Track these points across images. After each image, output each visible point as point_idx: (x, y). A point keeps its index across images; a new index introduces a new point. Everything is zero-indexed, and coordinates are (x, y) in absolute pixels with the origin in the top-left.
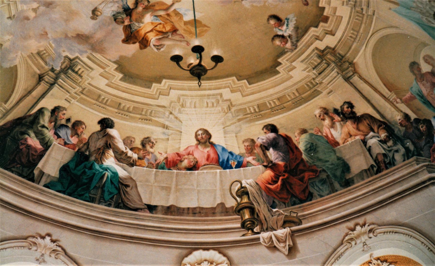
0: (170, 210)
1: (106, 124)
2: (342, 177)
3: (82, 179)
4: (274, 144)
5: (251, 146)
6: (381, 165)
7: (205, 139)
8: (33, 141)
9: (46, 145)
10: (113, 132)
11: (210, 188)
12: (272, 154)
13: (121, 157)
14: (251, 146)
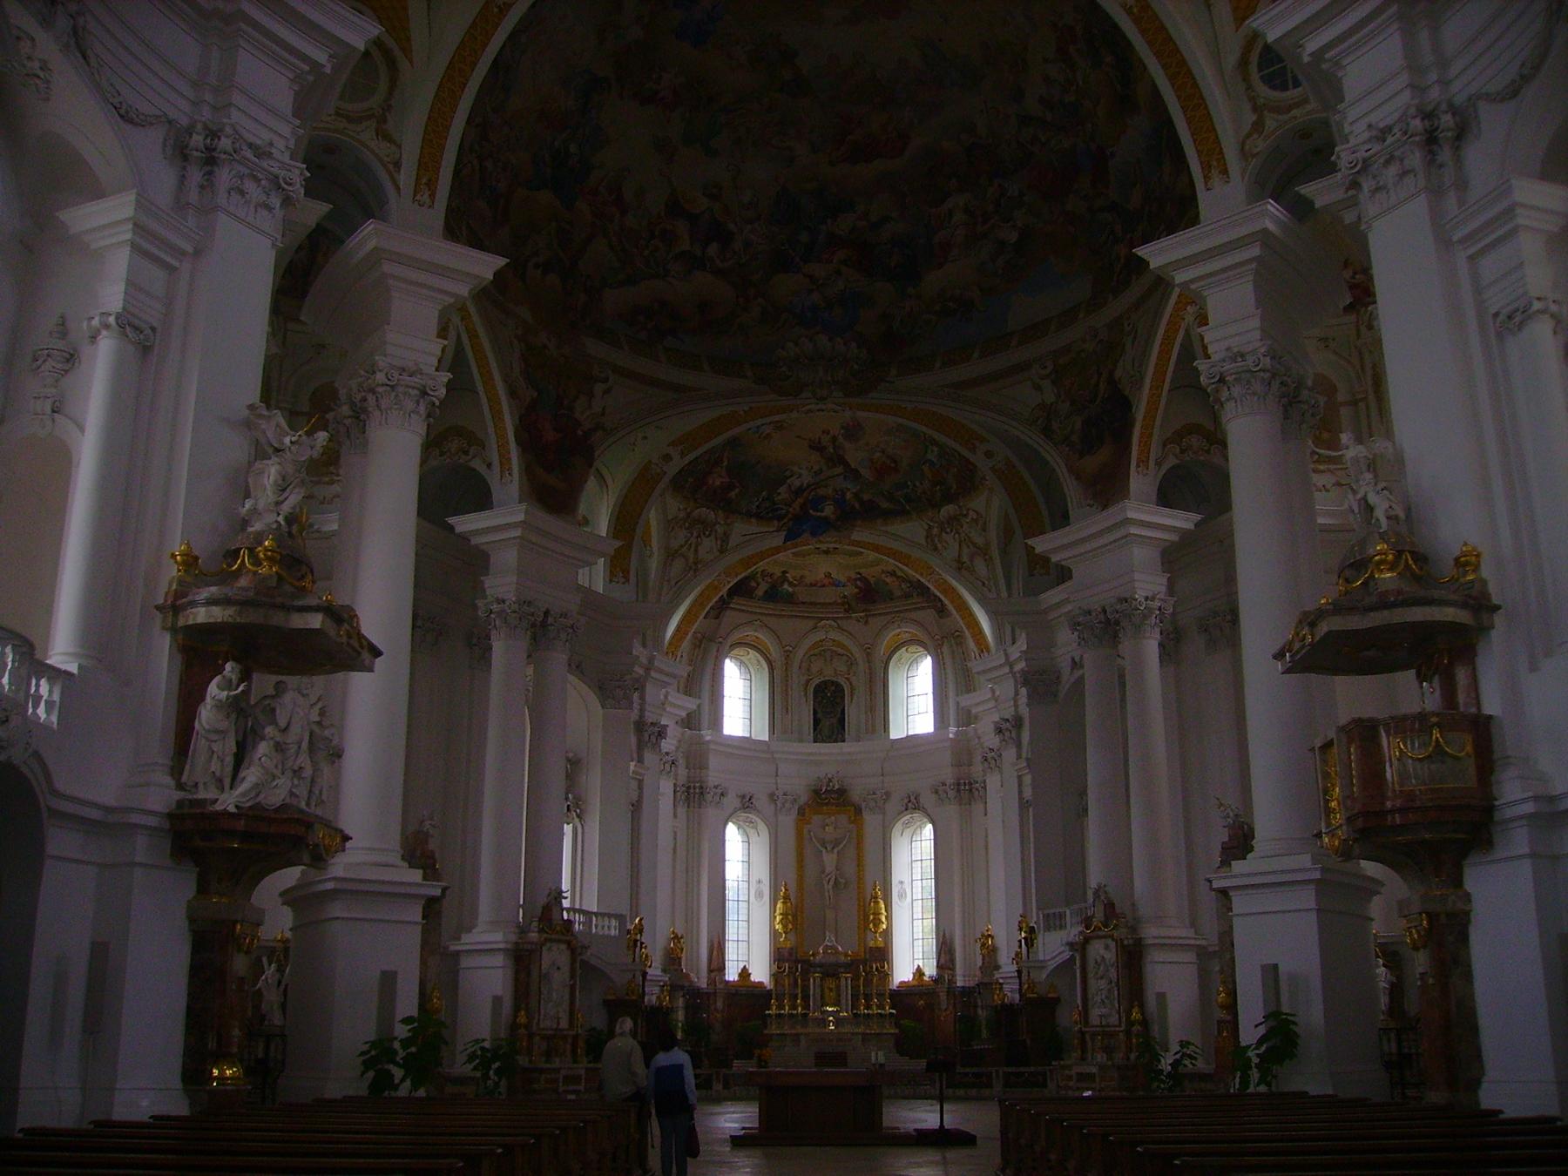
3: (773, 595)
6: (907, 596)
7: (828, 575)
8: (753, 584)
11: (829, 595)
13: (791, 584)
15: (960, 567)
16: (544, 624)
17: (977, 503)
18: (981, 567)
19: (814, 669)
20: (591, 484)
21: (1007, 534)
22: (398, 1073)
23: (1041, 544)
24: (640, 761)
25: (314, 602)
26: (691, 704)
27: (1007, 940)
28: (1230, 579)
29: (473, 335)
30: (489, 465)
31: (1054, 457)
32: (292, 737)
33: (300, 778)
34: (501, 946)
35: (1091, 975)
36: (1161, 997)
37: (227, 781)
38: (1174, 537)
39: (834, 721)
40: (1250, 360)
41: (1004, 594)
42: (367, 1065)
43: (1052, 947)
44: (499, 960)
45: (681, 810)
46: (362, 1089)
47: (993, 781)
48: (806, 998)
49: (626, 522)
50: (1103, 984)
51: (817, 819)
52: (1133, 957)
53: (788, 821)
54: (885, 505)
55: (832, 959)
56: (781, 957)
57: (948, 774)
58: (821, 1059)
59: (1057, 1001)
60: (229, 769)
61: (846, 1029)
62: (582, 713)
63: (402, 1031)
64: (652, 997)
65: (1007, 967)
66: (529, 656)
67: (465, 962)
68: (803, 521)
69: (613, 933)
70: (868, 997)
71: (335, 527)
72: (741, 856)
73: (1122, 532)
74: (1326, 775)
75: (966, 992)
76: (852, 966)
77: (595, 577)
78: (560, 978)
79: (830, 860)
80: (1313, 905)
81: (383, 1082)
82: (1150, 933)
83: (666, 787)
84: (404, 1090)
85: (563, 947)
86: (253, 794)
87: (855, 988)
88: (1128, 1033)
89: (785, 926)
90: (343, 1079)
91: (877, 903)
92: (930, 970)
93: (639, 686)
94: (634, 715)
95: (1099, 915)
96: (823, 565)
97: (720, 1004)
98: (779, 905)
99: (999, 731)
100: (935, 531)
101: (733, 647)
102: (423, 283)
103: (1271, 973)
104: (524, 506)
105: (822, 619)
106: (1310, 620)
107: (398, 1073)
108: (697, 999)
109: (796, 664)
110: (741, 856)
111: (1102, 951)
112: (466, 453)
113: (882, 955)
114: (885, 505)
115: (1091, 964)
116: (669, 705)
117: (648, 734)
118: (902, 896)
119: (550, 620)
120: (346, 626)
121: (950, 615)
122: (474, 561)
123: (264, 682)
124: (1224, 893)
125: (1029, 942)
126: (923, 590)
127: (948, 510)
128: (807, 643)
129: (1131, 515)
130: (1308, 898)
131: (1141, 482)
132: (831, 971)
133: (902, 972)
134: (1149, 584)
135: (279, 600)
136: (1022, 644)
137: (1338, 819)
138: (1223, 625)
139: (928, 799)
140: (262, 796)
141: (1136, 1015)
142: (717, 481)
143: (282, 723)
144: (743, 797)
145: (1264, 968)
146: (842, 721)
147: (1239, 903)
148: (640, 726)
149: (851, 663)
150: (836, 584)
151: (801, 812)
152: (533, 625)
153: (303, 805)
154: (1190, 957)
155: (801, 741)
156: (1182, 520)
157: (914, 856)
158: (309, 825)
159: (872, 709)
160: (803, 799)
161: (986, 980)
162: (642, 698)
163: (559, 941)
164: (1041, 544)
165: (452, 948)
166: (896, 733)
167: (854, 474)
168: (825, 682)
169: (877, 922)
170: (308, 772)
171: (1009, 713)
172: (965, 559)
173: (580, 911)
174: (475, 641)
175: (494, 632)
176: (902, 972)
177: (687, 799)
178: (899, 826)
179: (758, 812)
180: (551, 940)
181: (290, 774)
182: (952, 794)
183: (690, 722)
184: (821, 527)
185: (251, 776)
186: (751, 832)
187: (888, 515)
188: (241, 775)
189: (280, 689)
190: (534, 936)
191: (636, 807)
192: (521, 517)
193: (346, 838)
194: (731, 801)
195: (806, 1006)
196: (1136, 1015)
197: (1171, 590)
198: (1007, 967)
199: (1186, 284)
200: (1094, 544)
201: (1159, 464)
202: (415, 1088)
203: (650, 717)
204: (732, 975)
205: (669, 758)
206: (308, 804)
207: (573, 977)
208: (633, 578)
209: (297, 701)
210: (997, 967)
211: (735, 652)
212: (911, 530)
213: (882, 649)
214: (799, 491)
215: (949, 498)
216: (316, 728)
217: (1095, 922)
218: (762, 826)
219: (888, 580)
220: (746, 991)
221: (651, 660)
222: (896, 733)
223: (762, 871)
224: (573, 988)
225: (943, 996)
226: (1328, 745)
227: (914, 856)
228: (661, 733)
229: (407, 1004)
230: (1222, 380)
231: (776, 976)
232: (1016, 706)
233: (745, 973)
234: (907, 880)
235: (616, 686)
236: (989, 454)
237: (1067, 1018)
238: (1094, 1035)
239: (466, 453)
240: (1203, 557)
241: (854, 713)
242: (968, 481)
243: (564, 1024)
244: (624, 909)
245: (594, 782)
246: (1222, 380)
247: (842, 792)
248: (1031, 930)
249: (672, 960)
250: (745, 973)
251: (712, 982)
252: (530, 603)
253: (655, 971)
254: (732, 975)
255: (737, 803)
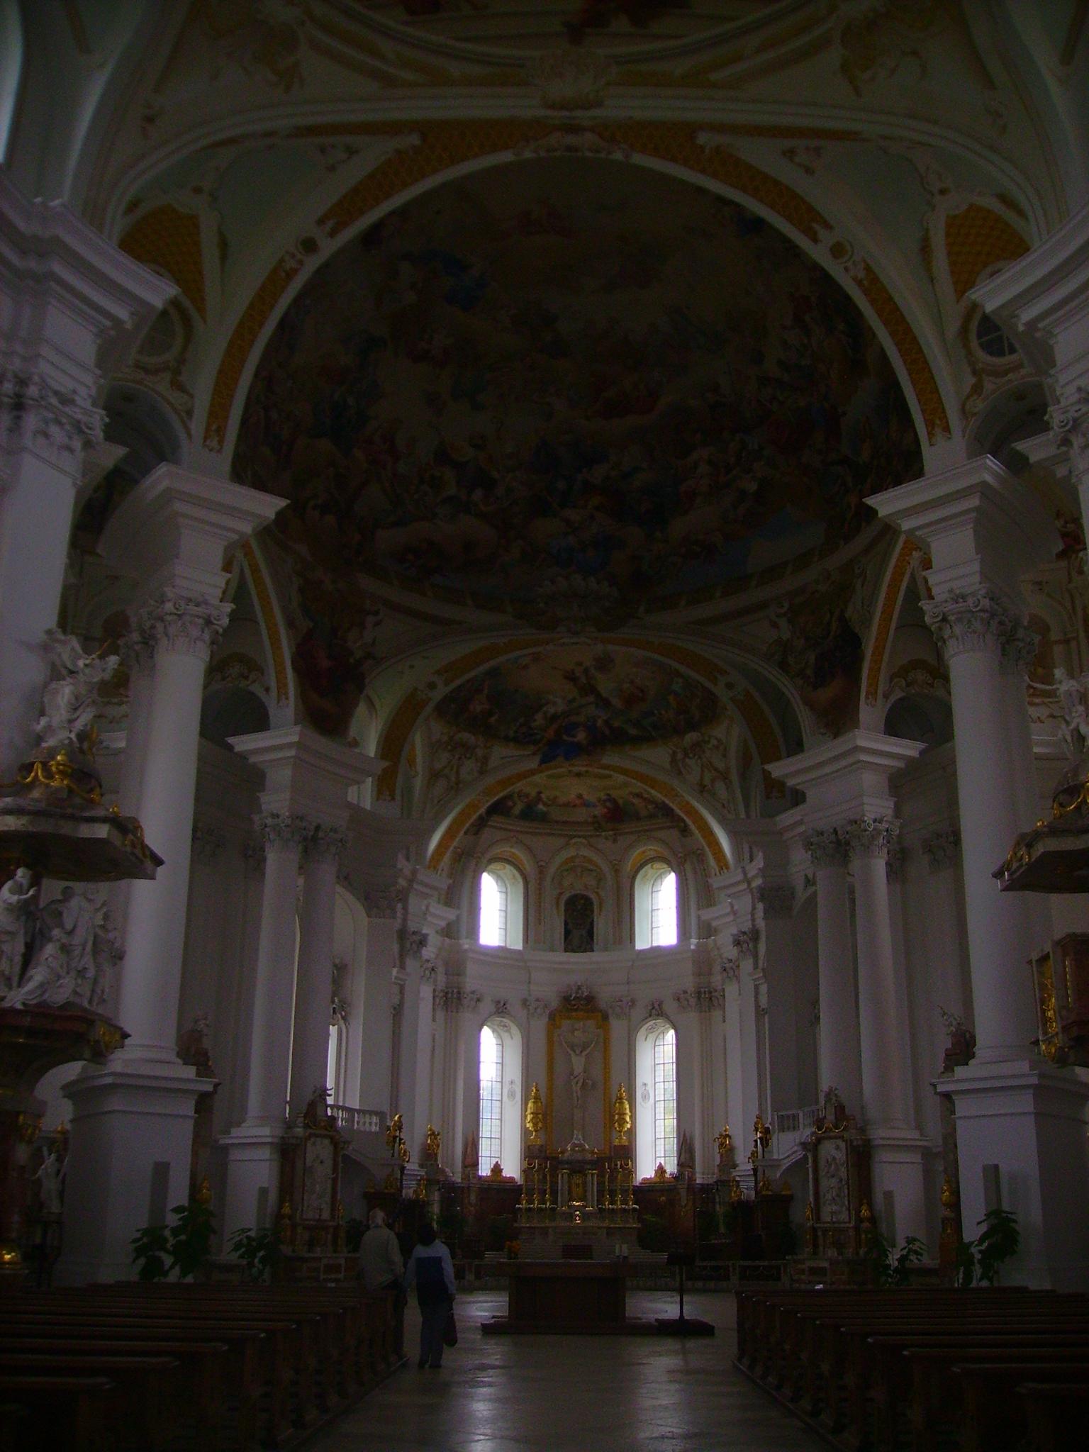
0: (565, 823)
1: (540, 793)
2: (638, 819)
3: (529, 814)
4: (609, 800)
5: (599, 800)
6: (652, 816)
7: (580, 796)
8: (510, 803)
9: (515, 804)
10: (543, 796)
11: (582, 814)
12: (608, 804)
13: (545, 804)
14: (599, 800)
15: (702, 789)
16: (314, 839)
17: (719, 731)
18: (720, 787)
19: (566, 883)
20: (361, 709)
21: (746, 760)
22: (168, 1260)
23: (778, 769)
24: (402, 967)
25: (101, 813)
26: (451, 914)
27: (744, 1142)
28: (952, 803)
29: (255, 570)
30: (267, 690)
31: (789, 688)
32: (77, 940)
33: (84, 977)
34: (269, 1140)
35: (822, 1173)
36: (889, 1195)
37: (15, 979)
38: (901, 764)
39: (584, 933)
40: (970, 601)
41: (743, 816)
42: (140, 1252)
43: (786, 1147)
44: (266, 1153)
45: (440, 1015)
46: (133, 1275)
47: (731, 990)
48: (554, 1193)
49: (393, 745)
50: (833, 1182)
51: (566, 1023)
52: (862, 1158)
53: (540, 1024)
54: (633, 731)
55: (579, 1156)
56: (531, 1154)
57: (689, 983)
58: (569, 1251)
59: (789, 1199)
60: (17, 969)
61: (592, 1223)
62: (348, 920)
63: (172, 1220)
64: (409, 1192)
65: (744, 1165)
66: (301, 868)
67: (235, 1155)
68: (559, 745)
69: (374, 1128)
70: (612, 1193)
71: (122, 744)
72: (495, 1057)
73: (851, 760)
74: (1043, 987)
75: (705, 1188)
76: (598, 1163)
77: (364, 794)
78: (323, 1171)
79: (578, 1063)
80: (1031, 1109)
81: (152, 1269)
82: (879, 1134)
83: (426, 992)
84: (173, 1277)
85: (327, 1142)
86: (39, 992)
87: (601, 1184)
88: (857, 1228)
89: (535, 1125)
90: (115, 1265)
91: (621, 1103)
92: (671, 1168)
93: (403, 897)
94: (397, 924)
95: (831, 1117)
96: (574, 786)
97: (473, 1198)
98: (530, 1105)
99: (737, 943)
100: (680, 756)
101: (491, 861)
102: (210, 520)
103: (992, 1173)
104: (298, 728)
105: (572, 837)
106: (1027, 841)
107: (168, 1260)
108: (452, 1193)
109: (549, 879)
110: (495, 1057)
111: (833, 1151)
112: (247, 678)
113: (627, 1153)
114: (633, 731)
115: (822, 1164)
116: (430, 916)
117: (409, 942)
118: (645, 1097)
119: (321, 834)
120: (131, 837)
121: (692, 834)
122: (251, 778)
123: (52, 888)
124: (947, 1096)
125: (765, 1141)
126: (668, 812)
127: (691, 737)
128: (559, 859)
129: (861, 743)
130: (1026, 1103)
131: (870, 713)
132: (578, 1168)
133: (645, 1170)
134: (877, 807)
135: (69, 811)
136: (759, 862)
137: (1055, 1027)
138: (946, 845)
139: (670, 1006)
140: (47, 995)
141: (864, 1212)
142: (478, 706)
143: (69, 927)
144: (499, 1002)
145: (985, 1168)
146: (591, 934)
147: (962, 1107)
148: (402, 934)
149: (600, 879)
150: (586, 804)
151: (552, 1017)
152: (305, 839)
153: (86, 1004)
154: (917, 1158)
155: (552, 950)
156: (909, 749)
157: (657, 1060)
158: (91, 1023)
159: (618, 923)
160: (555, 1004)
161: (724, 1178)
162: (405, 909)
163: (325, 1136)
164: (778, 769)
165: (222, 1142)
166: (641, 944)
167: (605, 703)
168: (575, 896)
169: (622, 1121)
170: (91, 973)
171: (747, 926)
172: (707, 781)
173: (344, 1108)
174: (250, 853)
175: (267, 845)
176: (645, 1170)
177: (446, 1003)
178: (643, 1031)
179: (513, 1018)
180: (317, 1136)
181: (73, 974)
182: (693, 1001)
183: (449, 931)
184: (574, 751)
185: (38, 975)
186: (505, 1035)
187: (637, 741)
188: (31, 972)
189: (67, 895)
190: (299, 1131)
191: (397, 1012)
192: (295, 738)
193: (125, 1036)
194: (487, 1006)
195: (554, 1202)
196: (864, 1212)
197: (898, 812)
198: (744, 1165)
199: (911, 532)
200: (827, 770)
201: (886, 696)
202: (184, 1273)
203: (412, 926)
204: (485, 1170)
205: (430, 965)
206: (90, 1002)
207: (335, 1169)
208: (398, 797)
209: (82, 906)
210: (735, 1166)
211: (492, 866)
212: (658, 755)
213: (628, 867)
214: (554, 718)
215: (692, 726)
216: (100, 932)
217: (828, 1124)
218: (515, 1030)
219: (636, 801)
220: (498, 1187)
221: (414, 872)
222: (641, 944)
223: (515, 1072)
224: (335, 1180)
225: (683, 1193)
226: (1044, 959)
227: (657, 1060)
228: (422, 942)
229: (178, 1194)
230: (944, 619)
231: (526, 1172)
232: (753, 920)
233: (497, 1169)
234: (650, 1082)
235: (381, 896)
236: (730, 686)
237: (800, 1214)
238: (825, 1231)
239: (247, 678)
240: (927, 781)
241: (602, 925)
242: (709, 711)
243: (326, 1215)
244: (386, 1108)
245: (358, 987)
246: (944, 619)
247: (590, 999)
248: (767, 1131)
249: (429, 1155)
250: (497, 1169)
251: (466, 1177)
252: (302, 818)
253: (412, 1166)
254: (485, 1170)
255: (493, 1009)
